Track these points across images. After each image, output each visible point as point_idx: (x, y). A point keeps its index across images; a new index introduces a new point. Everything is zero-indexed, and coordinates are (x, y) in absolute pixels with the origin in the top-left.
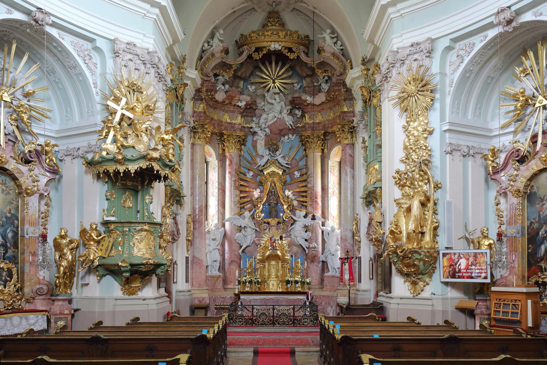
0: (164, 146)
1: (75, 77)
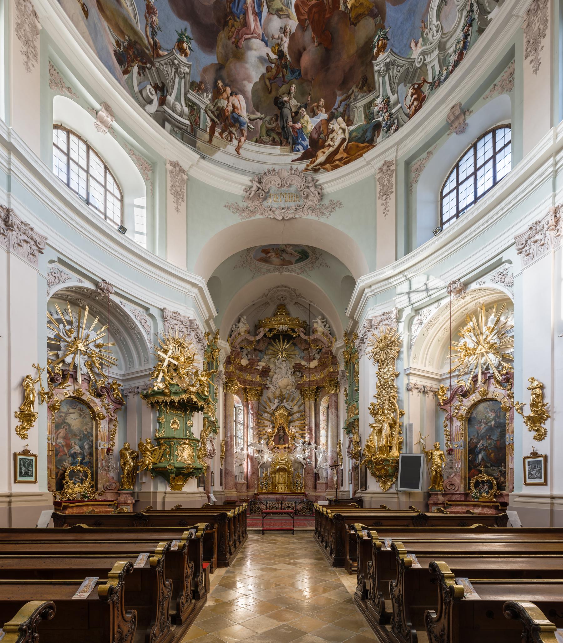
0: (201, 385)
1: (135, 336)
